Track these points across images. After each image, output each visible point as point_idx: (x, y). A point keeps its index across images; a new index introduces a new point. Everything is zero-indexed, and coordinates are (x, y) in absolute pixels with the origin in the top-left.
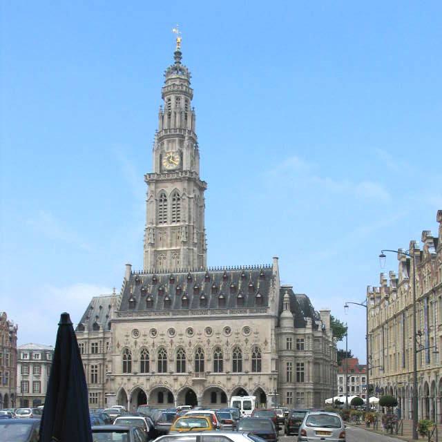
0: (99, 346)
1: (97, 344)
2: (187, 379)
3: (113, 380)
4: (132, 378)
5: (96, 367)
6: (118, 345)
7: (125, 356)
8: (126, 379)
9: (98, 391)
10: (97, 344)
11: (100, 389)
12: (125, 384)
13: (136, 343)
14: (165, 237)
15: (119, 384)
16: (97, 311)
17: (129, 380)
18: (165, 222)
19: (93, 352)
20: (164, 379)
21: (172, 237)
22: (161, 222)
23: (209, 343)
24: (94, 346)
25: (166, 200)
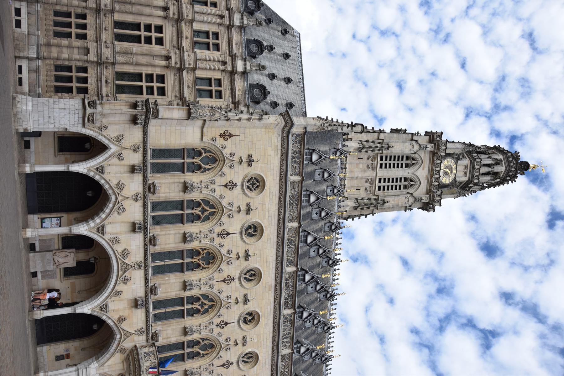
0: (212, 54)
1: (217, 47)
2: (140, 332)
3: (134, 120)
4: (138, 178)
5: (160, 41)
6: (227, 136)
7: (200, 154)
8: (136, 159)
9: (92, 46)
10: (217, 47)
11: (99, 55)
12: (120, 157)
13: (230, 186)
14: (361, 166)
15: (120, 139)
16: (282, 45)
17: (133, 169)
18: (381, 167)
19: (197, 33)
20: (138, 276)
21: (361, 179)
22: (382, 159)
23: (223, 365)
24: (211, 41)
25: (407, 166)
